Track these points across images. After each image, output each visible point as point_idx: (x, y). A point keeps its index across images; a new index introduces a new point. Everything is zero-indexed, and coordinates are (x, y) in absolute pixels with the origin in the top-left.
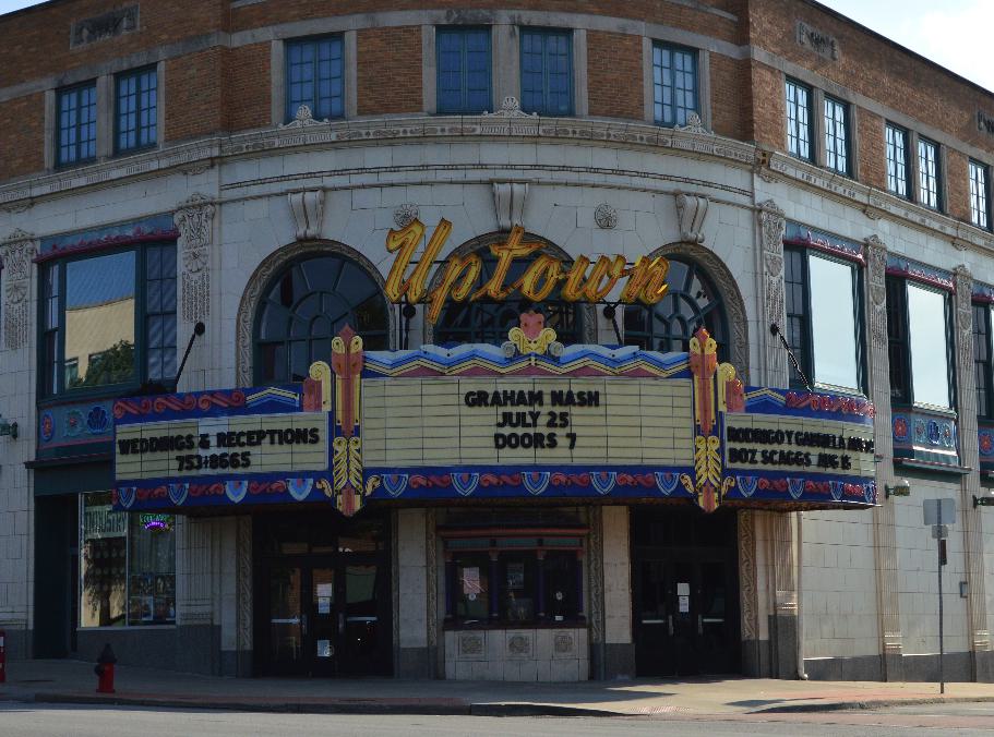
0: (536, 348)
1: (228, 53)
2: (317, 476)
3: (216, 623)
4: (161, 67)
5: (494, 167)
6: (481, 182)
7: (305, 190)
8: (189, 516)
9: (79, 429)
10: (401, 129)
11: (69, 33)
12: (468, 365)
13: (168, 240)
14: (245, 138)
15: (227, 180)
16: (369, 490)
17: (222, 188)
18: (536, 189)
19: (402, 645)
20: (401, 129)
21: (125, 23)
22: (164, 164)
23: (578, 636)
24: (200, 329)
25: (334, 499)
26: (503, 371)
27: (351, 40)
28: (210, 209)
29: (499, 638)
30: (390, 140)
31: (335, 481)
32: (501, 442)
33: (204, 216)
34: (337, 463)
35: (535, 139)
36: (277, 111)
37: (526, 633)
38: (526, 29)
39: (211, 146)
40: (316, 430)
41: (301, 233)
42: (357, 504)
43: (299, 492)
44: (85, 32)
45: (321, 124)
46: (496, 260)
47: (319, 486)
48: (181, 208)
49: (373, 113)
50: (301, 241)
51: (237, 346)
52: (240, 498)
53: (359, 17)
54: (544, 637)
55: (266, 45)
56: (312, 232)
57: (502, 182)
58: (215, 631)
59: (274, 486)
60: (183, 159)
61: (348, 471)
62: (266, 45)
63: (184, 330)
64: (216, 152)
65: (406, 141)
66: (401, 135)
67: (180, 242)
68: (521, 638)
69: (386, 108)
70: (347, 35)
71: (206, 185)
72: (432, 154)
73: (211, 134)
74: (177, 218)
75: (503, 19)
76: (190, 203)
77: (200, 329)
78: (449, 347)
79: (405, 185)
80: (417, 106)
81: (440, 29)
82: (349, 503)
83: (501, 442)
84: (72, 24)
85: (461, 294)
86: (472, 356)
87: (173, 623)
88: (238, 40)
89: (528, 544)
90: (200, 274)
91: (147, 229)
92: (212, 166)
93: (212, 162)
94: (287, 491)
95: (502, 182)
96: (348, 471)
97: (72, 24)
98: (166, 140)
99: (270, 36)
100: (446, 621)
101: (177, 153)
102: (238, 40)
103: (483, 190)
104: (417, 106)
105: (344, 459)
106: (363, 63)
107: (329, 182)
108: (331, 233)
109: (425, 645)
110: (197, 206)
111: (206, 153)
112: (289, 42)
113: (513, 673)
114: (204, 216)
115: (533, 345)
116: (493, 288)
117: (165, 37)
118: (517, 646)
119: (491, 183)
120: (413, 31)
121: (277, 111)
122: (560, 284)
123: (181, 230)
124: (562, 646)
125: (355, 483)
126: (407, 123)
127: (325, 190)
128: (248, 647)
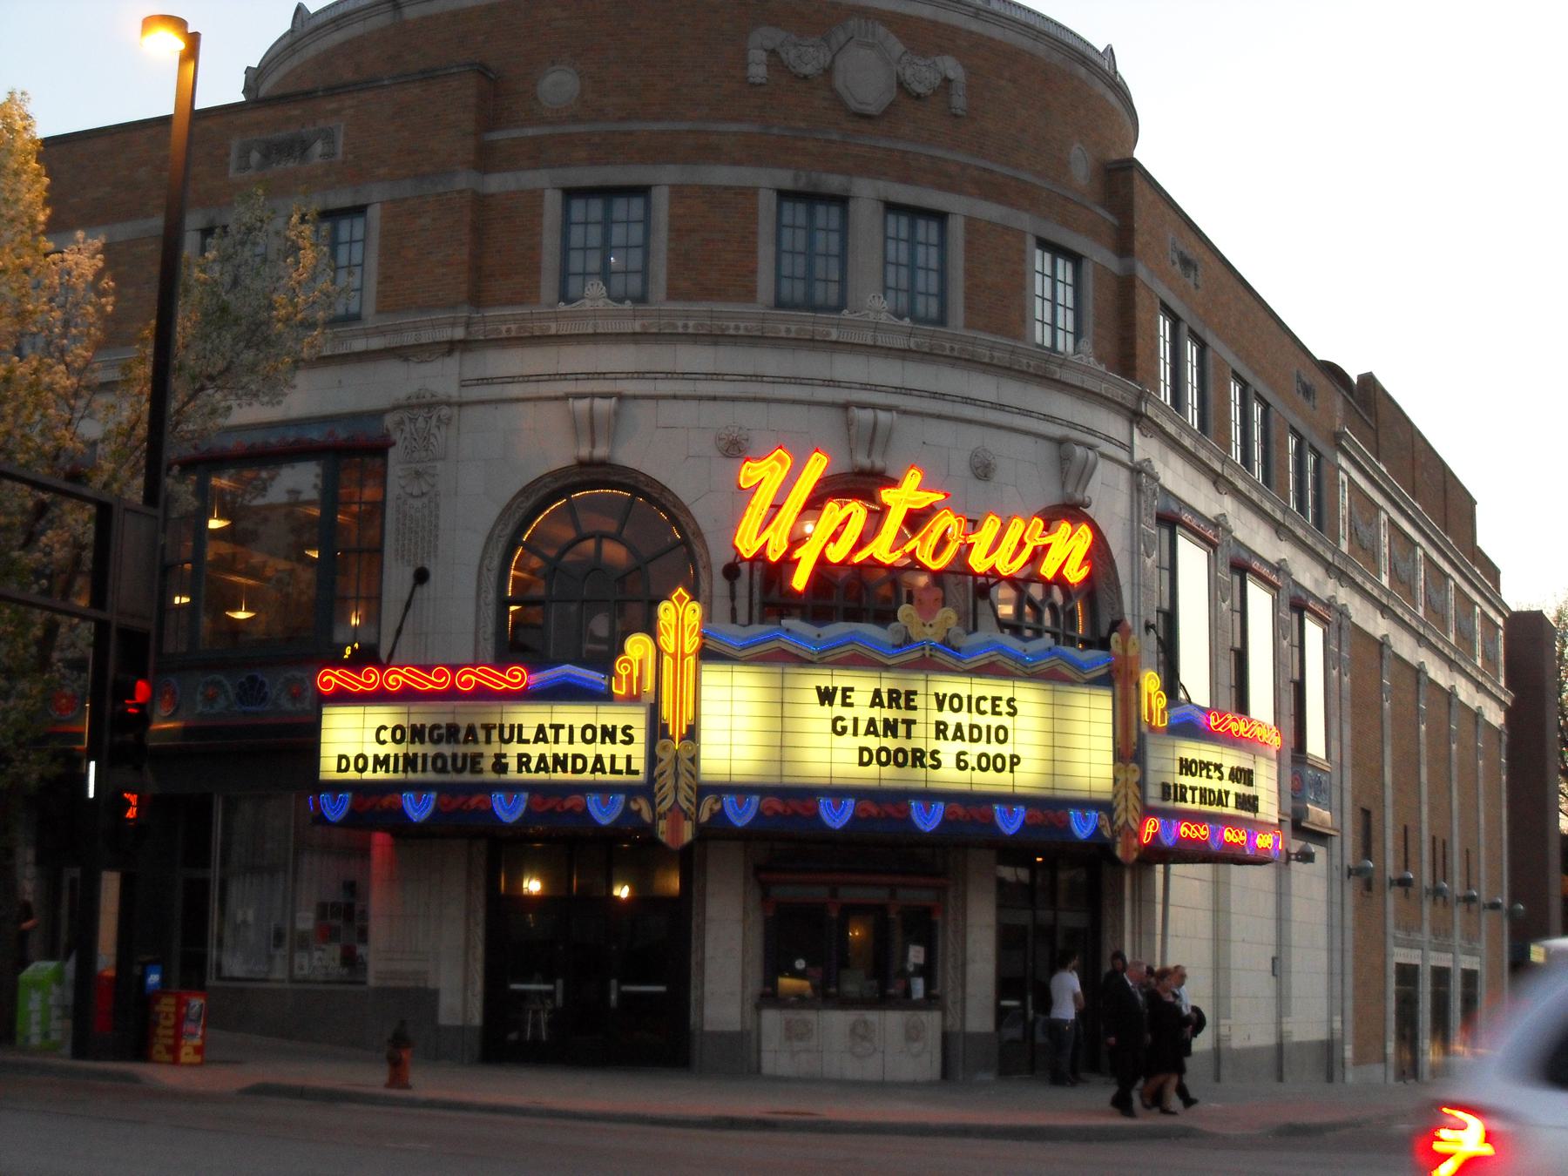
0: (932, 634)
1: (481, 202)
2: (630, 790)
3: (431, 985)
4: (374, 213)
5: (849, 386)
6: (833, 405)
7: (593, 396)
8: (395, 835)
9: (221, 704)
10: (732, 324)
11: (228, 155)
12: (846, 651)
13: (379, 449)
14: (502, 318)
15: (470, 373)
16: (705, 816)
17: (464, 384)
18: (906, 420)
19: (707, 1028)
20: (732, 324)
21: (318, 148)
22: (376, 343)
23: (931, 1021)
24: (421, 576)
25: (654, 823)
26: (890, 662)
27: (661, 198)
28: (445, 411)
29: (837, 1021)
30: (715, 338)
31: (657, 800)
32: (866, 757)
33: (434, 419)
34: (661, 774)
35: (904, 354)
36: (548, 285)
37: (872, 1016)
38: (891, 207)
39: (453, 325)
40: (630, 728)
41: (584, 452)
42: (687, 833)
43: (1081, 829)
44: (255, 157)
45: (620, 307)
46: (885, 509)
47: (634, 807)
48: (395, 408)
49: (688, 297)
50: (583, 464)
51: (478, 606)
52: (519, 814)
53: (671, 168)
54: (891, 1021)
55: (536, 196)
56: (601, 452)
57: (863, 406)
58: (427, 998)
59: (474, 802)
60: (409, 339)
61: (676, 788)
62: (536, 196)
63: (396, 579)
64: (459, 333)
65: (735, 340)
66: (732, 332)
67: (393, 454)
68: (865, 1022)
69: (707, 293)
70: (655, 192)
71: (441, 378)
72: (770, 362)
73: (454, 306)
74: (389, 421)
75: (867, 192)
76: (414, 401)
77: (421, 576)
78: (820, 625)
79: (733, 399)
80: (750, 294)
81: (783, 195)
82: (675, 830)
83: (866, 757)
84: (235, 144)
85: (836, 554)
86: (850, 640)
87: (364, 983)
88: (496, 183)
89: (877, 895)
90: (425, 500)
91: (342, 434)
92: (450, 352)
93: (451, 347)
94: (586, 811)
95: (863, 406)
96: (676, 788)
97: (235, 144)
98: (378, 312)
99: (544, 181)
100: (763, 995)
101: (398, 330)
102: (496, 183)
103: (834, 415)
104: (750, 294)
105: (670, 771)
106: (677, 232)
107: (629, 387)
108: (628, 455)
109: (738, 1027)
110: (425, 405)
111: (446, 334)
112: (571, 194)
113: (852, 1070)
114: (434, 419)
115: (928, 630)
116: (882, 549)
117: (382, 171)
118: (859, 1033)
119: (846, 406)
120: (750, 193)
121: (548, 285)
122: (1039, 554)
123: (397, 436)
124: (913, 1034)
125: (685, 805)
126: (731, 313)
127: (621, 397)
128: (477, 1019)
